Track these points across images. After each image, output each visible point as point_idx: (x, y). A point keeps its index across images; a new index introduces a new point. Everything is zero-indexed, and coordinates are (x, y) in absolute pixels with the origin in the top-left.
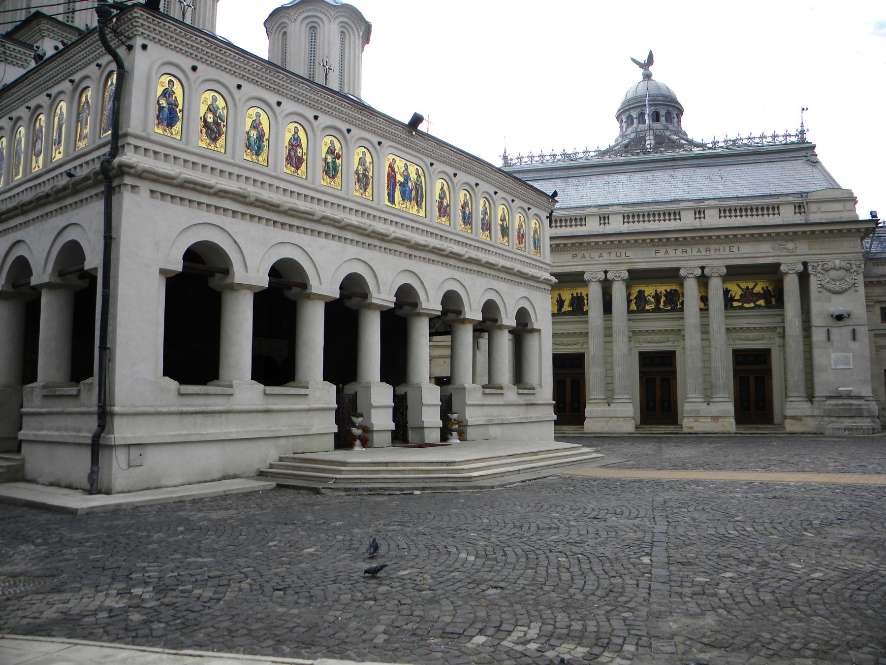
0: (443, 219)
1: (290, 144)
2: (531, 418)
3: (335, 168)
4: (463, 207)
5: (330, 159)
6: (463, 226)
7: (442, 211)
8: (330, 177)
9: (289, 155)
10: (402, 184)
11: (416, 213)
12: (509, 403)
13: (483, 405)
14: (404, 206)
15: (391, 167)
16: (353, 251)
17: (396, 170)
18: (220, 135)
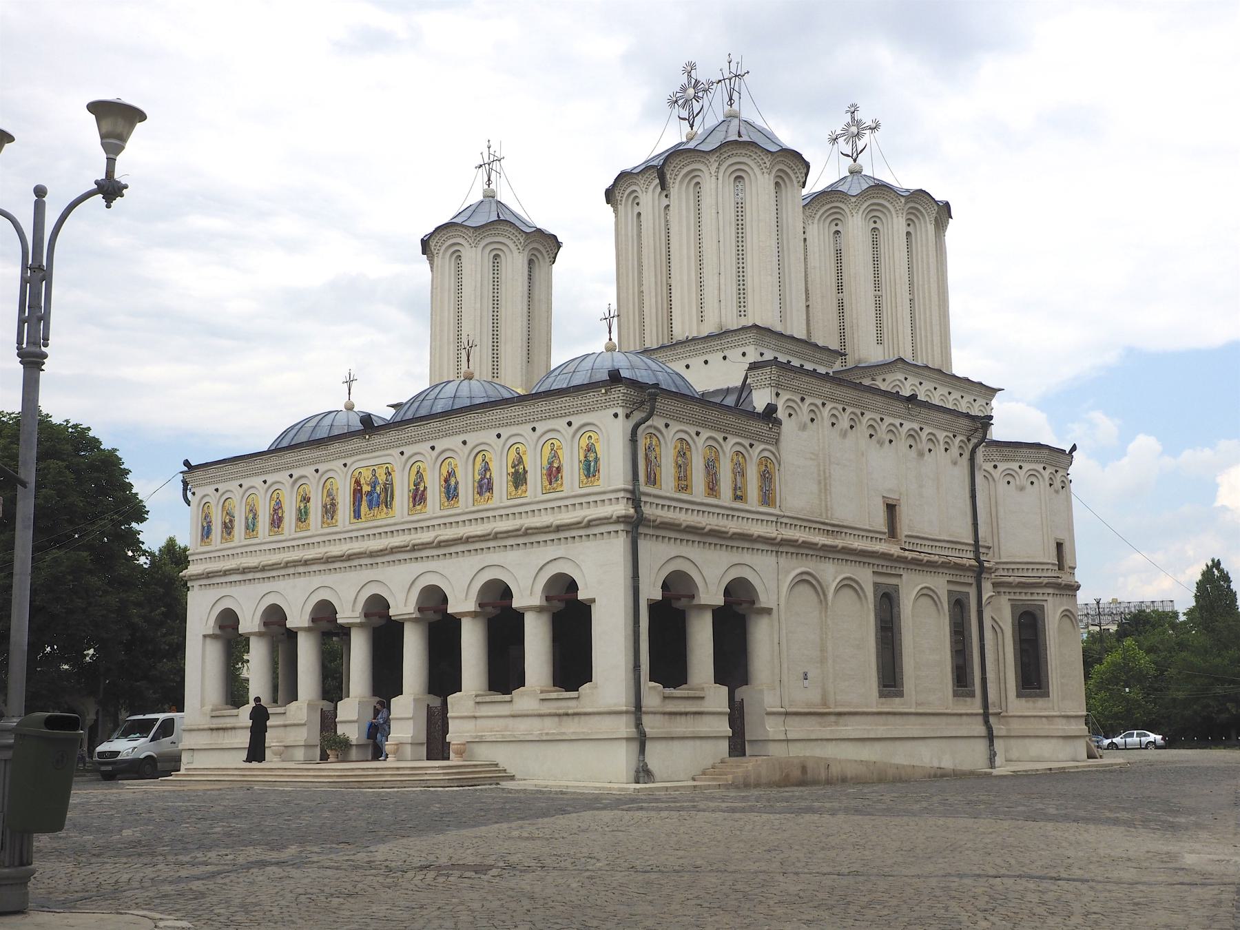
0: (418, 507)
1: (275, 510)
2: (564, 733)
3: (306, 513)
4: (446, 481)
5: (302, 506)
6: (446, 504)
7: (417, 499)
8: (302, 522)
9: (273, 520)
10: (369, 494)
11: (385, 516)
12: (526, 712)
13: (475, 717)
14: (371, 515)
15: (358, 482)
16: (317, 581)
17: (362, 481)
18: (233, 528)
